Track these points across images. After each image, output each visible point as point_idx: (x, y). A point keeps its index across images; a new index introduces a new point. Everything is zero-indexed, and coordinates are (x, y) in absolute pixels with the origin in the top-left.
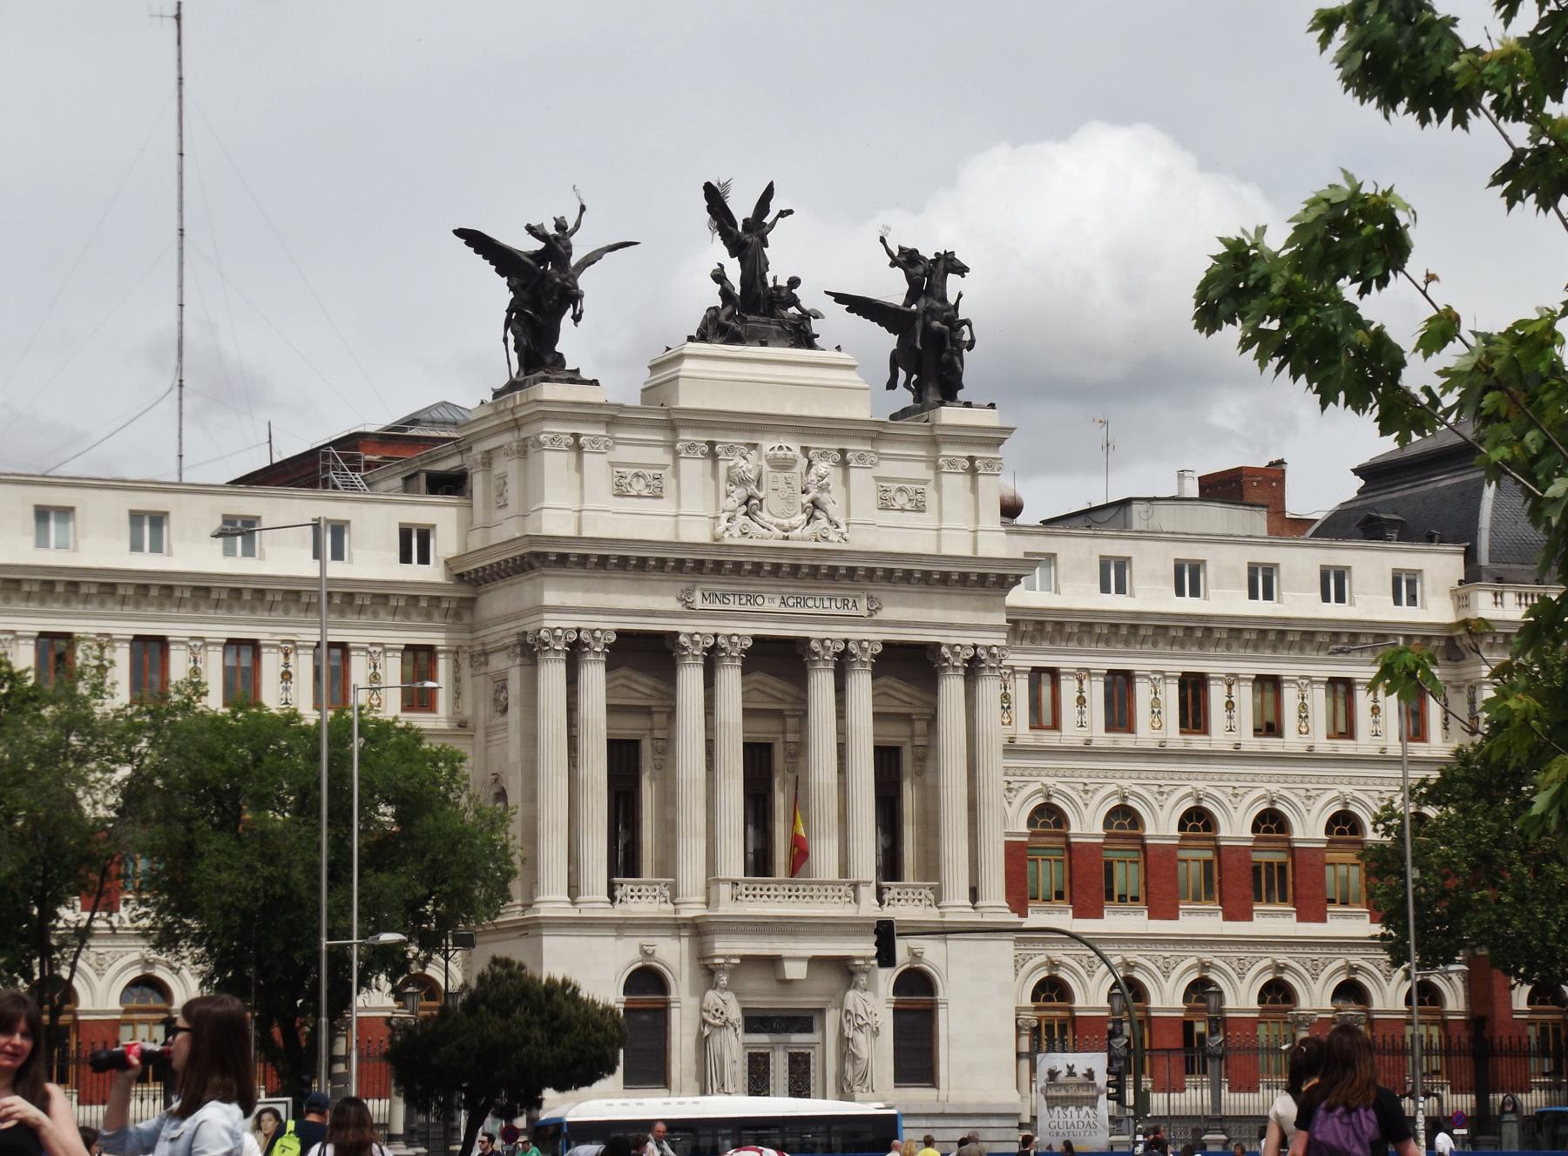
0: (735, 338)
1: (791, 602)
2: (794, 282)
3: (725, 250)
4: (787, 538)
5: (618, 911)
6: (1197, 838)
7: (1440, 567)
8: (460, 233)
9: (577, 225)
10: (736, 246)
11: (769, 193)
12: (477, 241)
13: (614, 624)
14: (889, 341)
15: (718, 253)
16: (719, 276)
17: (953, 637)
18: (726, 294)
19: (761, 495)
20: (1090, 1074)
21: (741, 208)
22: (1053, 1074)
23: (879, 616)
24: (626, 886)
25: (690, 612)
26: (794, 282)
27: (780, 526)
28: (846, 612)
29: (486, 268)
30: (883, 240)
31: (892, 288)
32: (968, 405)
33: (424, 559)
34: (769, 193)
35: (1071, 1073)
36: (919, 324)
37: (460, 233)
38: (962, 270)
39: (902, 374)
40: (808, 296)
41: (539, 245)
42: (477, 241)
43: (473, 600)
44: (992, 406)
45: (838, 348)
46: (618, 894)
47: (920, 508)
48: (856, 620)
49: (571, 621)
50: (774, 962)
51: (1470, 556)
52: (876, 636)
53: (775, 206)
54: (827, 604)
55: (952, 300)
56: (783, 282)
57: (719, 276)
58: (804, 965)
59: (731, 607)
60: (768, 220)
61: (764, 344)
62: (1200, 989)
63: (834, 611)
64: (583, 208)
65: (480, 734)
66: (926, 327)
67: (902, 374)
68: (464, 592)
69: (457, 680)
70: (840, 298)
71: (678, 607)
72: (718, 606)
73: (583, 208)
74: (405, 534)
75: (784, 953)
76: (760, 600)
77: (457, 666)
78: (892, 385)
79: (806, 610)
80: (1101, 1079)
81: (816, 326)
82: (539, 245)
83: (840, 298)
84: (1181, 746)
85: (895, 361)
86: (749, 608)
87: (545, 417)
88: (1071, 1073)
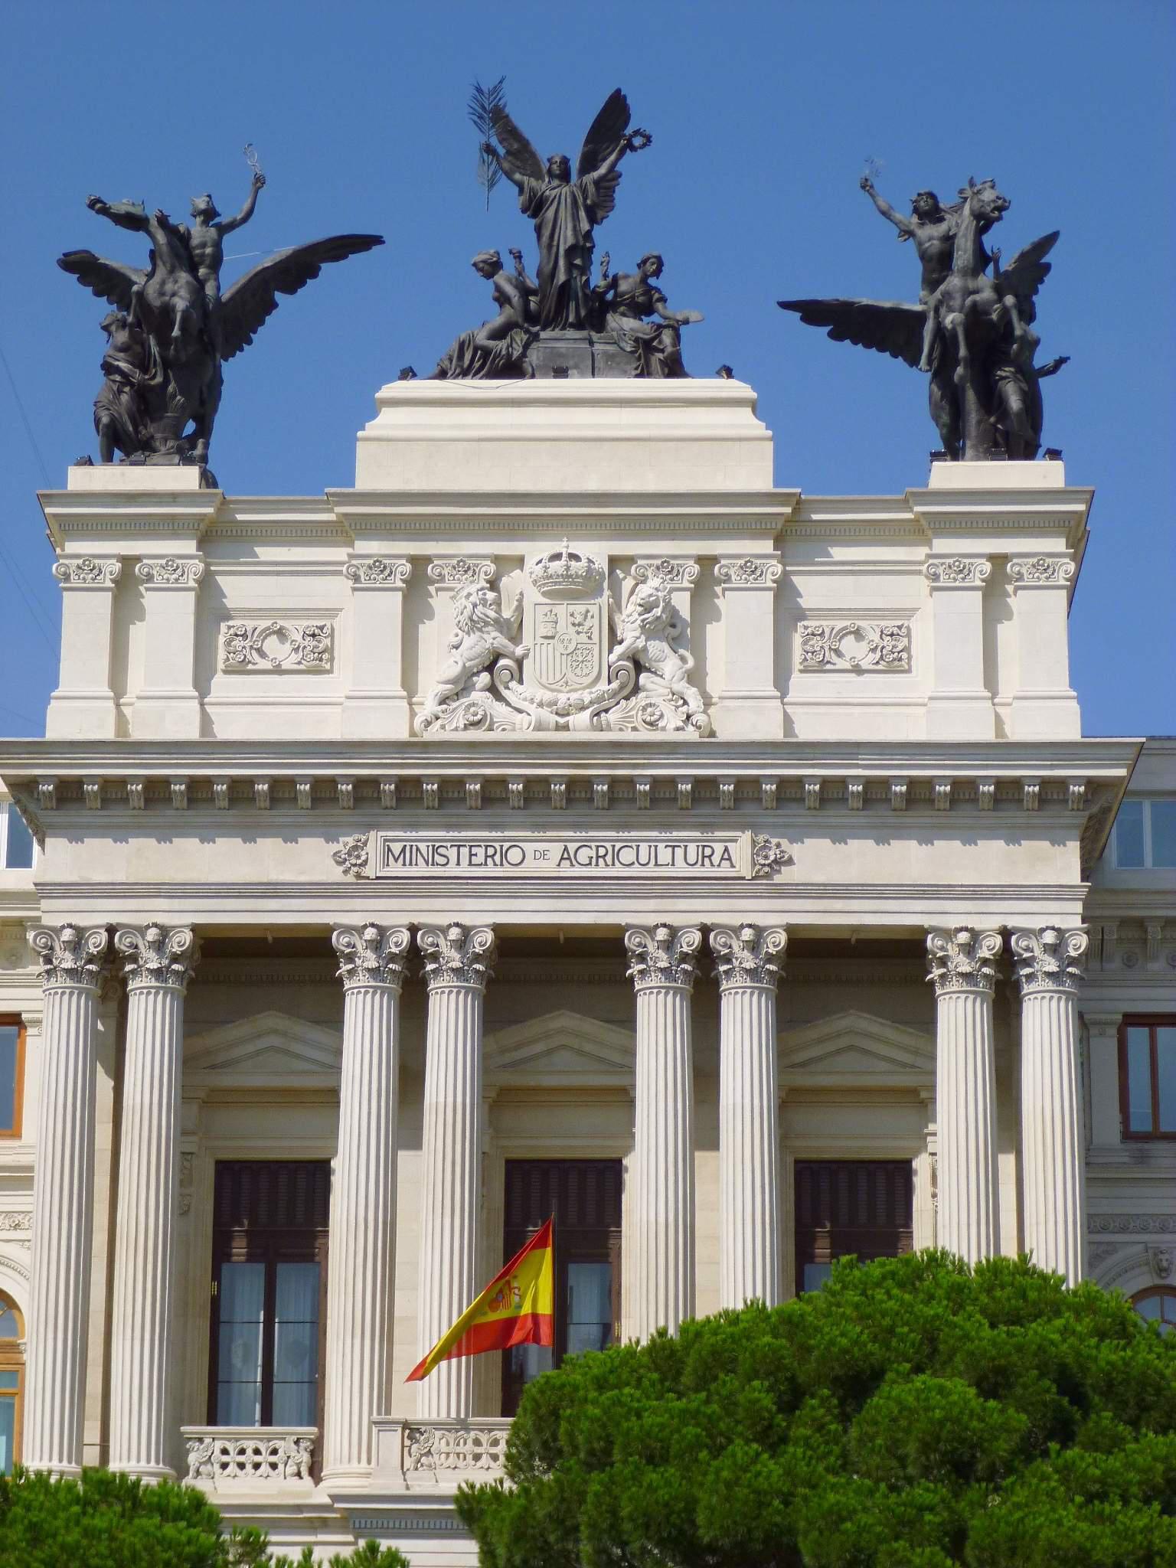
0: (512, 369)
1: (584, 855)
4: (566, 728)
9: (250, 213)
11: (616, 110)
12: (85, 268)
13: (183, 918)
17: (955, 915)
19: (519, 651)
24: (208, 1444)
25: (364, 886)
27: (548, 702)
28: (707, 871)
30: (866, 186)
34: (616, 110)
42: (85, 268)
45: (729, 373)
48: (726, 886)
49: (96, 915)
52: (777, 917)
54: (664, 855)
59: (452, 870)
61: (561, 372)
63: (681, 869)
64: (259, 181)
66: (939, 329)
70: (812, 312)
71: (336, 874)
72: (421, 870)
73: (259, 181)
76: (514, 855)
79: (617, 871)
83: (812, 312)
86: (490, 871)
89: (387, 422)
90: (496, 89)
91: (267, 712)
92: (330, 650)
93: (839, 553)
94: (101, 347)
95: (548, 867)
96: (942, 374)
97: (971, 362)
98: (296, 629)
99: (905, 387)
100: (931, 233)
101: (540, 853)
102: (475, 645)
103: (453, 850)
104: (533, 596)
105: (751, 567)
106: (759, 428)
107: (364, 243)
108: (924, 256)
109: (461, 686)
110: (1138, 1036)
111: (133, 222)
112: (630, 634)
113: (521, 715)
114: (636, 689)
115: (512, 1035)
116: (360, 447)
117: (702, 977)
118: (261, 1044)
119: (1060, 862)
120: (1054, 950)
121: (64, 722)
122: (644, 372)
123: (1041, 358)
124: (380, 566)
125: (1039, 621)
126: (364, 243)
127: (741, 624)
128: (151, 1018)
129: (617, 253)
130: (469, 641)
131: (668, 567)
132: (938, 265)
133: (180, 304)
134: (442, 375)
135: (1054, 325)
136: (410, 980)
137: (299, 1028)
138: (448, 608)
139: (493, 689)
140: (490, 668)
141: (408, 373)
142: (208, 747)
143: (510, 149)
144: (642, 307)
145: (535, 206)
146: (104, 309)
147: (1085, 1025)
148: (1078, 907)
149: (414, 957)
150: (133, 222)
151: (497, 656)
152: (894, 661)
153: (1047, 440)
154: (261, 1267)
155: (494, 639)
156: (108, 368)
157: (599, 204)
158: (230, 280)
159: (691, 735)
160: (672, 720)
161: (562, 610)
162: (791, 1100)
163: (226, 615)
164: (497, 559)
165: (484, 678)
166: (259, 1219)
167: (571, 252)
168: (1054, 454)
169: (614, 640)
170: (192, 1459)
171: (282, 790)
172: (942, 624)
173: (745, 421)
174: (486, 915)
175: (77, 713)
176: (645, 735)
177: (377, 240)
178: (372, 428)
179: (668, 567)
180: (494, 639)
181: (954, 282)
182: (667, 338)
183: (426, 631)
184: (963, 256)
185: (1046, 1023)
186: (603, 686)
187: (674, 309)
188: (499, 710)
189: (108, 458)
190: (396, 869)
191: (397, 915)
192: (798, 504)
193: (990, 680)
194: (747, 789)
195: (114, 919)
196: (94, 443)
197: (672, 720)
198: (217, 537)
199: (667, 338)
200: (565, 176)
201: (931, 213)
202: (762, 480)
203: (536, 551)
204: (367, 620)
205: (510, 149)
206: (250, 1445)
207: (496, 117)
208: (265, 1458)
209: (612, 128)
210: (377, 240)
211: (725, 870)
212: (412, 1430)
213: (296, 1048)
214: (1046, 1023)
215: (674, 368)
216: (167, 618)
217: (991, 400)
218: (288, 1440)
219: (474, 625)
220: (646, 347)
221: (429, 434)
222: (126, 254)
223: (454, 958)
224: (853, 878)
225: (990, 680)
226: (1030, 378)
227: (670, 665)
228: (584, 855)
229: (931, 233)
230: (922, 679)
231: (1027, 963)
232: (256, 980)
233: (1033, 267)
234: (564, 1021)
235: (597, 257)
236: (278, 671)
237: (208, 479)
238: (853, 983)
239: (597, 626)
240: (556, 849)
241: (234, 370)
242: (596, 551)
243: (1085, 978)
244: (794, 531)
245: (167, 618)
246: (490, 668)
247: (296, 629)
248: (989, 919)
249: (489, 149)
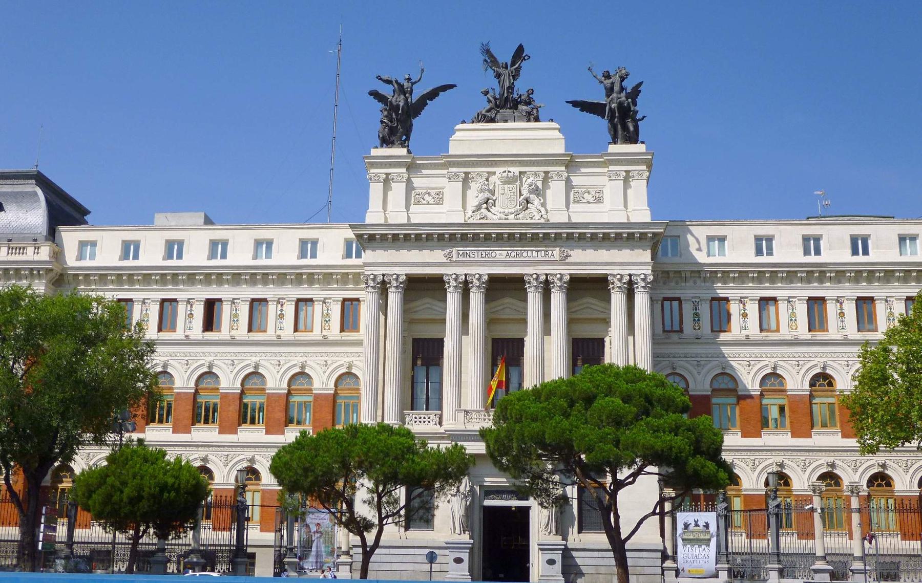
0: (492, 120)
1: (513, 255)
6: (824, 391)
11: (520, 49)
12: (375, 94)
13: (403, 272)
17: (616, 270)
20: (707, 526)
22: (686, 526)
23: (569, 260)
24: (411, 416)
25: (451, 263)
27: (503, 212)
28: (547, 259)
34: (520, 49)
35: (697, 525)
42: (375, 94)
45: (552, 120)
49: (379, 271)
52: (567, 271)
54: (535, 254)
61: (506, 121)
63: (540, 258)
64: (423, 70)
66: (610, 108)
70: (575, 104)
71: (444, 260)
73: (423, 70)
76: (493, 254)
80: (713, 528)
83: (575, 104)
84: (809, 337)
87: (373, 165)
88: (697, 525)
89: (458, 135)
90: (487, 44)
91: (425, 215)
92: (442, 198)
93: (583, 170)
94: (380, 116)
95: (503, 258)
96: (611, 120)
97: (619, 117)
98: (433, 192)
99: (602, 124)
100: (608, 82)
101: (501, 254)
102: (482, 196)
103: (477, 253)
104: (498, 183)
105: (559, 174)
106: (561, 136)
107: (452, 86)
108: (606, 88)
109: (478, 208)
110: (667, 303)
111: (389, 82)
112: (525, 193)
113: (495, 215)
114: (527, 208)
115: (493, 304)
116: (451, 143)
117: (546, 288)
118: (425, 306)
119: (645, 256)
120: (644, 280)
121: (370, 219)
122: (529, 121)
123: (639, 116)
124: (456, 175)
125: (639, 188)
126: (452, 86)
127: (556, 189)
128: (394, 299)
129: (521, 87)
130: (480, 195)
131: (536, 174)
132: (610, 91)
133: (401, 104)
134: (473, 122)
135: (642, 107)
136: (465, 289)
138: (474, 186)
139: (487, 209)
140: (486, 203)
141: (464, 122)
142: (409, 225)
143: (491, 61)
144: (528, 103)
145: (498, 76)
146: (381, 106)
147: (652, 300)
148: (650, 268)
149: (466, 283)
150: (389, 82)
151: (489, 199)
152: (599, 200)
153: (640, 139)
154: (425, 368)
156: (382, 122)
157: (516, 75)
158: (415, 97)
159: (542, 221)
160: (537, 217)
161: (506, 186)
162: (571, 321)
163: (414, 189)
164: (488, 173)
165: (485, 205)
166: (424, 354)
167: (508, 88)
168: (643, 143)
169: (521, 195)
170: (407, 420)
171: (429, 237)
172: (612, 190)
173: (557, 134)
174: (486, 271)
175: (374, 216)
176: (530, 221)
177: (455, 86)
178: (453, 137)
179: (536, 174)
181: (614, 95)
182: (535, 111)
183: (469, 192)
184: (617, 88)
185: (641, 300)
186: (518, 207)
187: (537, 104)
188: (489, 214)
189: (382, 146)
190: (461, 258)
191: (461, 271)
192: (572, 157)
193: (626, 206)
194: (558, 235)
195: (384, 272)
196: (378, 142)
198: (412, 168)
199: (535, 111)
200: (506, 68)
201: (607, 76)
202: (562, 150)
203: (499, 170)
205: (491, 61)
206: (423, 416)
207: (488, 52)
208: (427, 420)
209: (519, 54)
210: (455, 86)
211: (552, 258)
212: (467, 412)
213: (434, 307)
214: (641, 300)
215: (537, 120)
216: (398, 190)
217: (625, 128)
218: (433, 414)
219: (482, 191)
220: (529, 114)
221: (469, 138)
222: (387, 91)
223: (477, 283)
224: (588, 260)
225: (626, 206)
226: (636, 122)
227: (536, 201)
228: (513, 255)
229: (608, 82)
230: (607, 204)
231: (636, 283)
232: (423, 288)
233: (636, 91)
234: (507, 300)
235: (515, 89)
236: (428, 204)
237: (409, 152)
238: (588, 288)
241: (416, 122)
242: (516, 170)
243: (653, 287)
244: (571, 164)
245: (398, 190)
246: (486, 203)
247: (433, 192)
249: (485, 60)
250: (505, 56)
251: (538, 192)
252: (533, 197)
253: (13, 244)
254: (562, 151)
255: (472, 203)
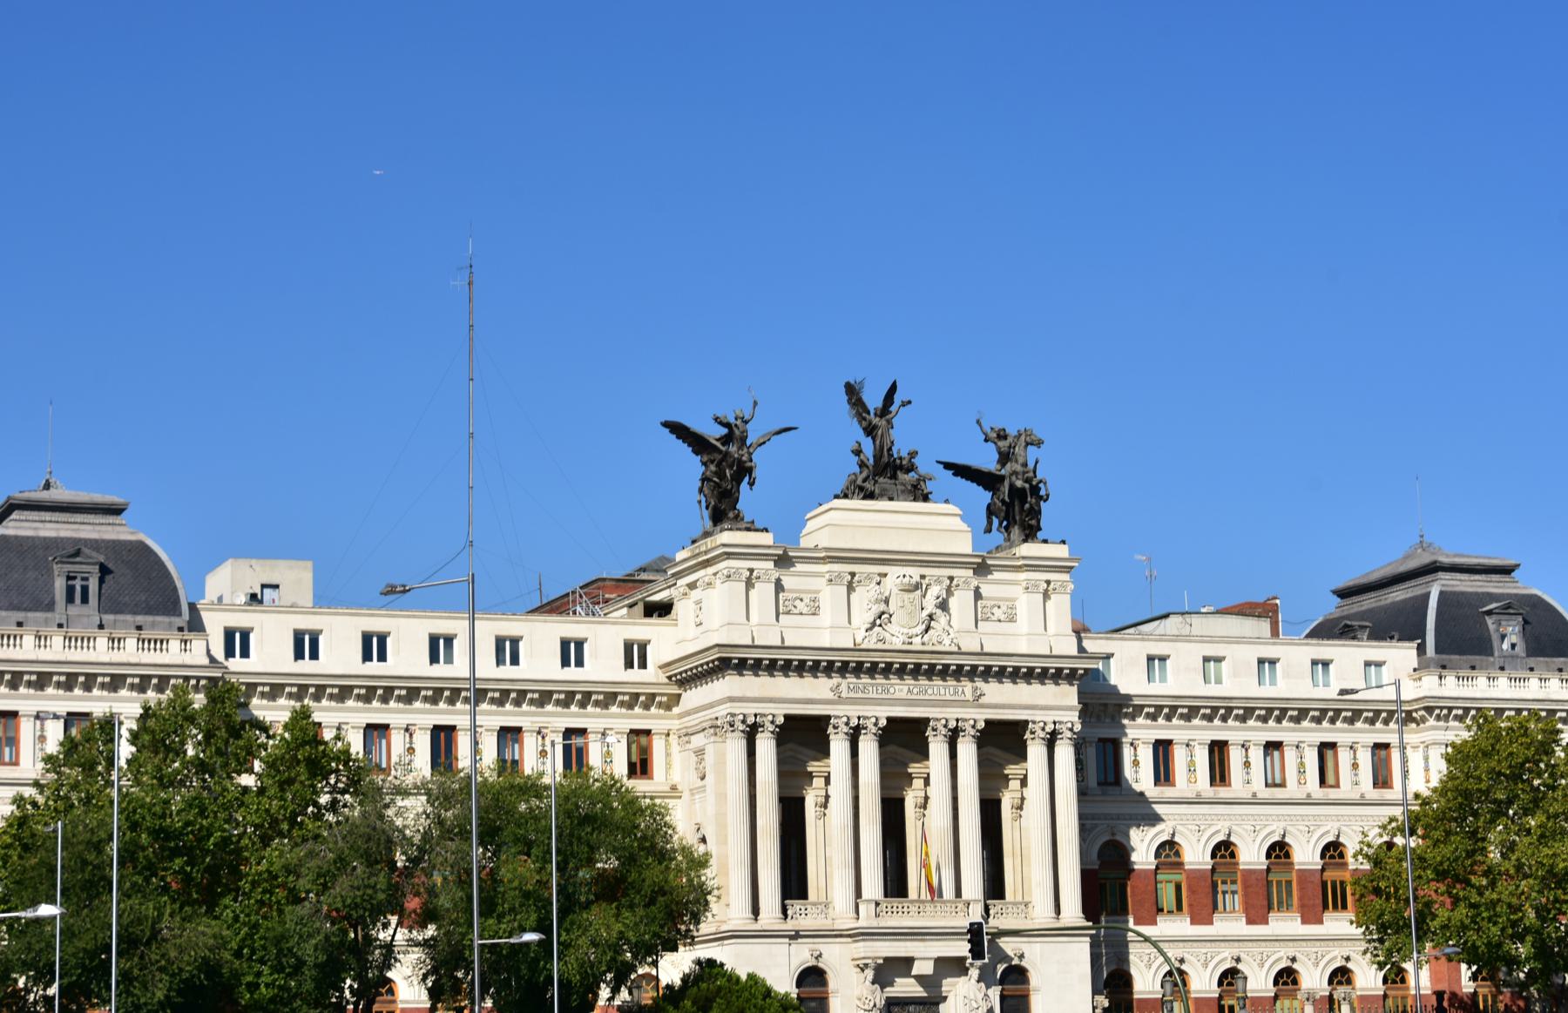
0: (870, 496)
2: (913, 454)
3: (861, 432)
5: (790, 925)
7: (1400, 657)
8: (666, 424)
10: (870, 431)
11: (893, 389)
13: (780, 712)
14: (983, 497)
15: (859, 434)
16: (858, 452)
17: (1038, 716)
18: (862, 465)
21: (873, 400)
23: (983, 700)
24: (795, 906)
25: (840, 700)
26: (913, 454)
29: (684, 450)
31: (986, 459)
32: (1045, 541)
33: (643, 665)
34: (893, 389)
36: (1007, 483)
37: (666, 424)
38: (1039, 443)
39: (996, 521)
40: (925, 465)
41: (725, 431)
43: (679, 696)
44: (1064, 542)
45: (947, 501)
46: (790, 912)
47: (1012, 619)
48: (963, 703)
49: (750, 709)
50: (908, 962)
51: (1421, 649)
52: (981, 716)
53: (898, 398)
55: (1031, 466)
56: (904, 454)
57: (858, 452)
58: (932, 963)
60: (893, 409)
61: (891, 499)
62: (1230, 977)
63: (948, 697)
64: (755, 403)
65: (686, 795)
67: (996, 521)
68: (675, 690)
69: (668, 755)
70: (948, 466)
71: (830, 695)
72: (860, 695)
73: (755, 403)
74: (367, 638)
75: (915, 955)
77: (667, 744)
78: (988, 530)
81: (929, 487)
82: (725, 431)
83: (948, 466)
84: (1211, 795)
85: (990, 511)
104: (895, 591)
106: (964, 527)
113: (898, 636)
122: (915, 500)
124: (839, 576)
127: (961, 602)
128: (766, 747)
132: (1005, 458)
134: (846, 496)
136: (854, 736)
137: (801, 749)
141: (837, 497)
152: (1012, 619)
155: (883, 607)
160: (947, 641)
161: (906, 595)
172: (1027, 605)
173: (957, 523)
174: (883, 713)
180: (883, 607)
190: (852, 695)
191: (853, 712)
192: (984, 558)
197: (947, 641)
201: (1002, 435)
202: (967, 548)
203: (894, 572)
204: (832, 597)
214: (1065, 754)
215: (926, 498)
216: (763, 593)
219: (877, 601)
220: (915, 487)
232: (803, 737)
238: (1002, 741)
239: (917, 602)
240: (905, 689)
242: (915, 573)
244: (982, 569)
248: (1050, 717)
250: (873, 400)
251: (943, 606)
252: (939, 611)
253: (145, 634)
254: (969, 551)
255: (862, 617)
